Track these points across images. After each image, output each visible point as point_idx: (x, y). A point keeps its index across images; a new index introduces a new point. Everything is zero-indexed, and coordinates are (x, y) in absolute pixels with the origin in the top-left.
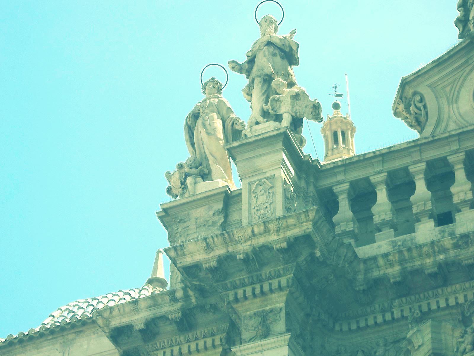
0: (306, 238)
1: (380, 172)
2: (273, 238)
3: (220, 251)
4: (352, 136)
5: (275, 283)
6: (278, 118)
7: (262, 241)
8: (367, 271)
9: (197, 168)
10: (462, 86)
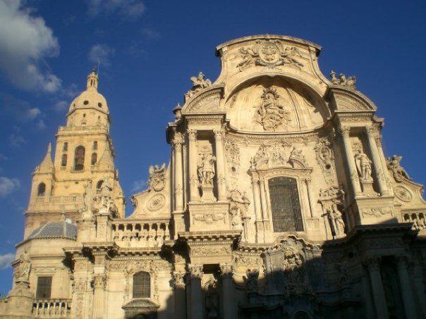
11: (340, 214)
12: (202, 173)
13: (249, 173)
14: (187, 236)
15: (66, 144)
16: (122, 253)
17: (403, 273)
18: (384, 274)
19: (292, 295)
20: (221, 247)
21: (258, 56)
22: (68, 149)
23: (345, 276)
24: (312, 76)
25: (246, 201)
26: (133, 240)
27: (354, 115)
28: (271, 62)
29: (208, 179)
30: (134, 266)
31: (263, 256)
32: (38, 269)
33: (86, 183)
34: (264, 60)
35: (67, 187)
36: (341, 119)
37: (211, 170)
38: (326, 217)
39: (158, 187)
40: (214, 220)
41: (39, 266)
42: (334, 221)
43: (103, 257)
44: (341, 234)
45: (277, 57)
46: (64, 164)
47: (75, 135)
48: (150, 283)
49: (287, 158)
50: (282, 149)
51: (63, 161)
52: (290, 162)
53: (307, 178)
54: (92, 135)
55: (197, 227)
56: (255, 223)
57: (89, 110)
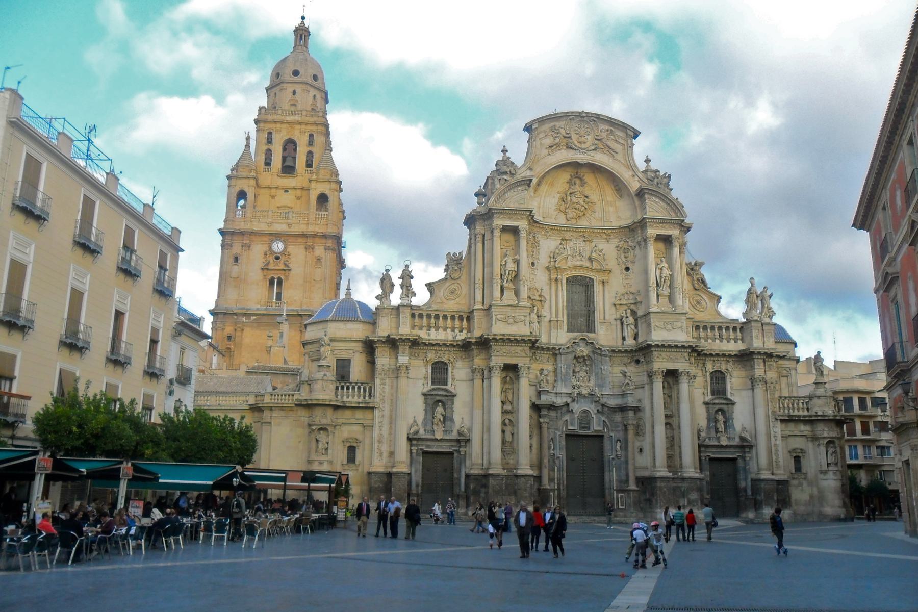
6: (408, 297)
7: (408, 337)
11: (631, 320)
12: (505, 271)
13: (548, 268)
14: (490, 337)
15: (270, 134)
16: (422, 343)
17: (684, 386)
18: (666, 384)
19: (579, 394)
20: (521, 348)
21: (570, 137)
22: (274, 141)
23: (630, 382)
24: (624, 165)
25: (543, 299)
26: (433, 330)
27: (662, 222)
28: (583, 146)
30: (432, 356)
31: (555, 355)
32: (336, 352)
33: (299, 193)
34: (576, 142)
35: (273, 197)
36: (648, 224)
37: (513, 269)
38: (619, 321)
39: (456, 275)
41: (336, 348)
42: (625, 327)
43: (407, 347)
44: (630, 342)
45: (590, 138)
46: (268, 163)
48: (447, 372)
49: (587, 255)
50: (583, 244)
51: (266, 159)
52: (590, 259)
53: (605, 279)
54: (307, 124)
55: (499, 329)
56: (550, 321)
57: (301, 85)
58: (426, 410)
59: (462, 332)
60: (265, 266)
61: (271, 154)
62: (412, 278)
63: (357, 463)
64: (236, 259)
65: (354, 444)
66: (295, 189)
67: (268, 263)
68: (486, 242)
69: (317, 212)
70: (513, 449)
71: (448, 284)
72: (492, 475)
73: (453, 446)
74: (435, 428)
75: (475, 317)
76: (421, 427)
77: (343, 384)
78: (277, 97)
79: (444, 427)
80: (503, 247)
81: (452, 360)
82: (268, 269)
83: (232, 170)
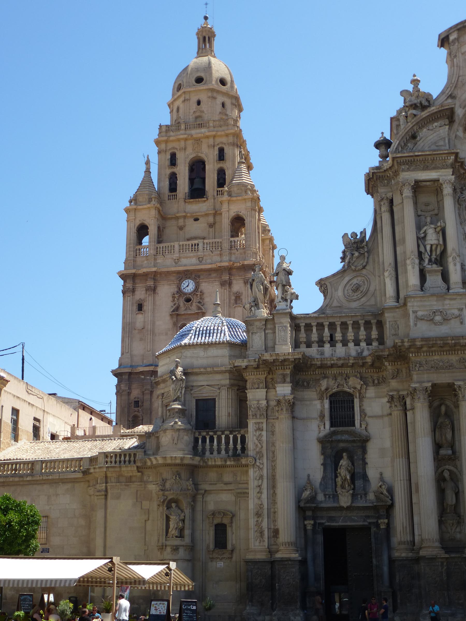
0: (300, 359)
1: (315, 322)
2: (290, 357)
3: (274, 358)
4: (214, 40)
5: (288, 367)
6: (286, 300)
7: (287, 357)
8: (311, 361)
9: (254, 302)
10: (340, 285)
26: (327, 346)
29: (434, 256)
35: (181, 228)
37: (436, 242)
40: (444, 319)
41: (195, 384)
43: (288, 372)
46: (173, 188)
47: (186, 140)
51: (170, 184)
58: (324, 464)
59: (371, 345)
60: (173, 311)
61: (176, 178)
62: (289, 273)
63: (229, 547)
64: (140, 307)
65: (226, 521)
66: (207, 215)
67: (177, 309)
68: (395, 209)
69: (232, 239)
70: (459, 516)
71: (347, 279)
72: (424, 558)
73: (368, 517)
74: (339, 490)
75: (388, 320)
76: (319, 491)
77: (204, 434)
78: (181, 111)
79: (354, 489)
80: (420, 213)
81: (359, 387)
82: (178, 315)
83: (130, 202)
